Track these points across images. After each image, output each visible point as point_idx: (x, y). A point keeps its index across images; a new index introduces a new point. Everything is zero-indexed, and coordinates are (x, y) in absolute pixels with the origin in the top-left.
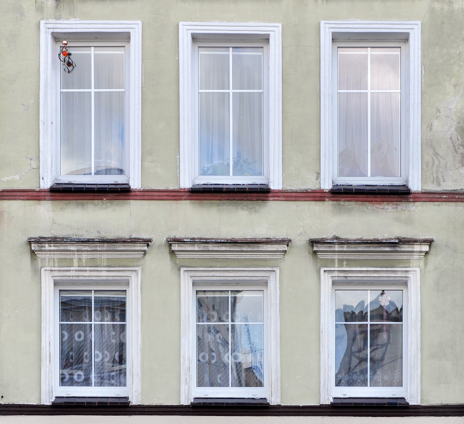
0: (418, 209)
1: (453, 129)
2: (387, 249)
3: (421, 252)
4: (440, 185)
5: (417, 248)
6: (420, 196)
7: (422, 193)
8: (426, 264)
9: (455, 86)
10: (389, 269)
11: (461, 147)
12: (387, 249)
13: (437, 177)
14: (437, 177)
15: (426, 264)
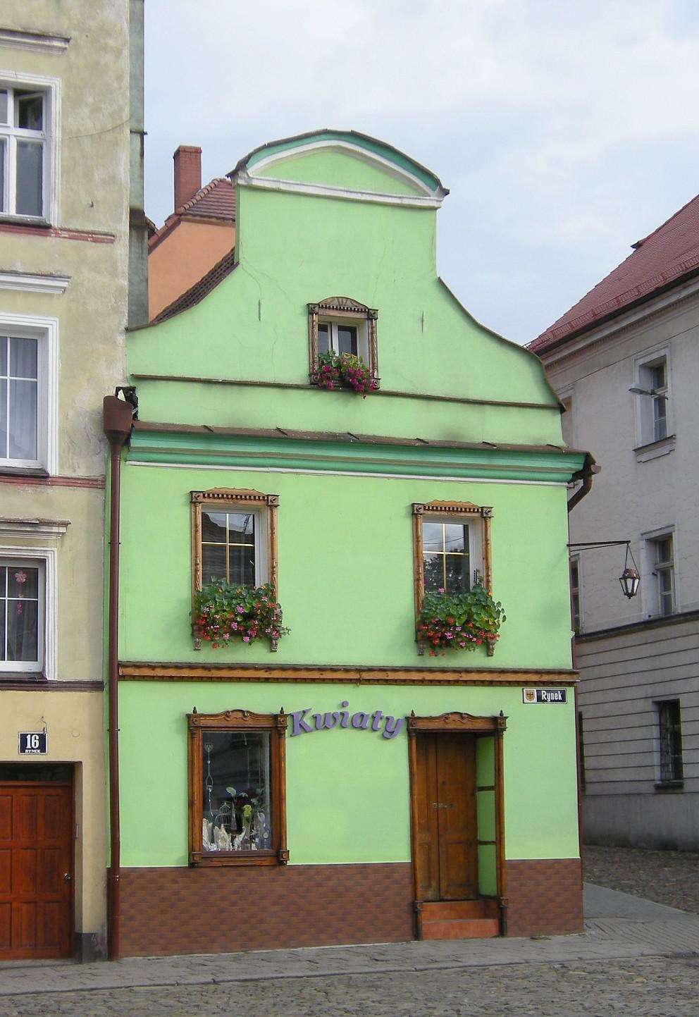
0: (56, 493)
1: (87, 419)
2: (28, 529)
3: (59, 533)
4: (75, 471)
5: (55, 529)
6: (58, 480)
7: (60, 477)
8: (62, 545)
9: (88, 380)
10: (30, 548)
11: (94, 437)
12: (28, 529)
13: (73, 464)
14: (73, 464)
15: (62, 545)
